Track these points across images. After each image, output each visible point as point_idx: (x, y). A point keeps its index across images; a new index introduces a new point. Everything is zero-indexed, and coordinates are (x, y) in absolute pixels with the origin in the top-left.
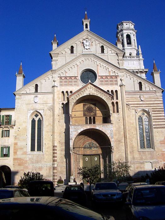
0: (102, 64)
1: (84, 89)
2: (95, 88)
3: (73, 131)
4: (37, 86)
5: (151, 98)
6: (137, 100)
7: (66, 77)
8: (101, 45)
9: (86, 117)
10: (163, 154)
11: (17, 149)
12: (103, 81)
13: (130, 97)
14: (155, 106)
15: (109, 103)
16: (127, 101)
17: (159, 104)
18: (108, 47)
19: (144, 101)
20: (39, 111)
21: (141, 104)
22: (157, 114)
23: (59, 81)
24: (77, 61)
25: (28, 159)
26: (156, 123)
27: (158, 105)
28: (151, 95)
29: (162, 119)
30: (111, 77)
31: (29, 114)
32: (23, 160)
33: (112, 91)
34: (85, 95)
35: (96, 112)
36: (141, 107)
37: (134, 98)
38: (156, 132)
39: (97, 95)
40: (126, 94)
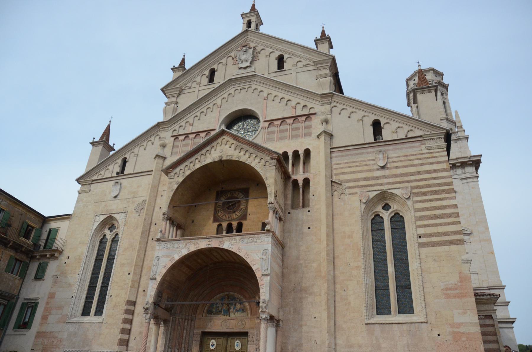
0: (274, 93)
1: (208, 148)
2: (234, 142)
3: (163, 256)
4: (125, 161)
5: (409, 158)
6: (366, 168)
7: (187, 135)
8: (277, 54)
9: (220, 226)
10: (458, 333)
11: (51, 310)
12: (273, 132)
13: (346, 161)
14: (422, 180)
15: (268, 175)
16: (337, 174)
17: (435, 171)
18: (295, 55)
19: (388, 168)
20: (114, 215)
21: (377, 178)
22: (431, 200)
23: (172, 145)
24: (219, 96)
25: (65, 336)
26: (429, 230)
27: (434, 175)
28: (410, 150)
29: (449, 215)
30: (295, 118)
31: (97, 224)
32: (55, 337)
33: (296, 154)
34: (208, 161)
35: (246, 209)
36: (378, 185)
37: (357, 164)
38: (426, 257)
39: (239, 157)
40: (334, 155)
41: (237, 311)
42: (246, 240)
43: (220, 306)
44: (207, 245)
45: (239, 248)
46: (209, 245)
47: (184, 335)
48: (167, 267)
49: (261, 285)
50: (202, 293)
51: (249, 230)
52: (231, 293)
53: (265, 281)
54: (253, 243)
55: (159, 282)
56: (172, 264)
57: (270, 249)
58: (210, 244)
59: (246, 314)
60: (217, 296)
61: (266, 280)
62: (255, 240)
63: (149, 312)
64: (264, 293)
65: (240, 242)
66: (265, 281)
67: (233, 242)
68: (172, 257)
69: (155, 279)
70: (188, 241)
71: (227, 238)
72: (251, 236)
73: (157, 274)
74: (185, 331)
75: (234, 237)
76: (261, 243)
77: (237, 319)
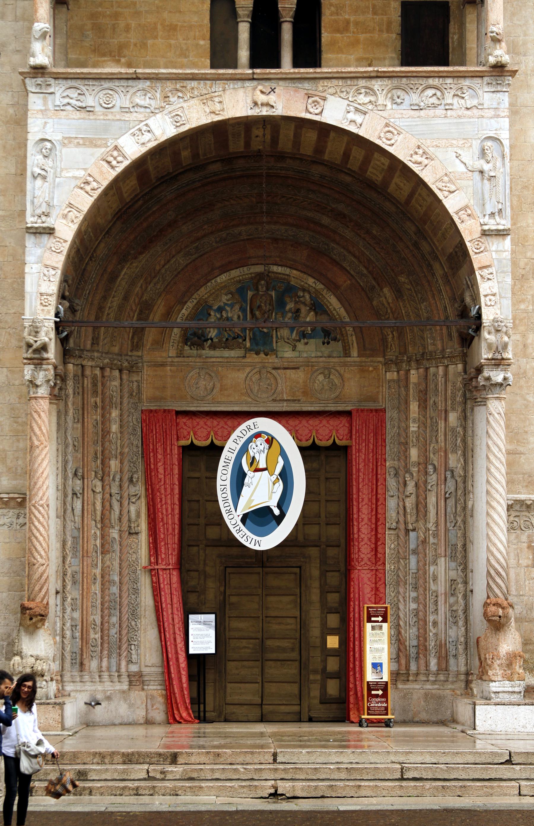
3: (67, 141)
41: (304, 335)
42: (414, 98)
44: (256, 104)
45: (387, 125)
46: (262, 105)
47: (114, 428)
48: (94, 185)
49: (480, 268)
50: (163, 266)
51: (352, 27)
52: (275, 268)
53: (494, 253)
54: (440, 111)
55: (67, 246)
56: (114, 174)
57: (505, 136)
58: (267, 105)
59: (341, 349)
61: (496, 251)
62: (449, 99)
63: (48, 359)
64: (494, 295)
65: (389, 106)
66: (494, 253)
67: (363, 99)
68: (111, 144)
69: (50, 231)
70: (170, 85)
71: (335, 82)
72: (431, 81)
73: (54, 213)
74: (115, 413)
75: (362, 83)
76: (468, 113)
77: (308, 364)
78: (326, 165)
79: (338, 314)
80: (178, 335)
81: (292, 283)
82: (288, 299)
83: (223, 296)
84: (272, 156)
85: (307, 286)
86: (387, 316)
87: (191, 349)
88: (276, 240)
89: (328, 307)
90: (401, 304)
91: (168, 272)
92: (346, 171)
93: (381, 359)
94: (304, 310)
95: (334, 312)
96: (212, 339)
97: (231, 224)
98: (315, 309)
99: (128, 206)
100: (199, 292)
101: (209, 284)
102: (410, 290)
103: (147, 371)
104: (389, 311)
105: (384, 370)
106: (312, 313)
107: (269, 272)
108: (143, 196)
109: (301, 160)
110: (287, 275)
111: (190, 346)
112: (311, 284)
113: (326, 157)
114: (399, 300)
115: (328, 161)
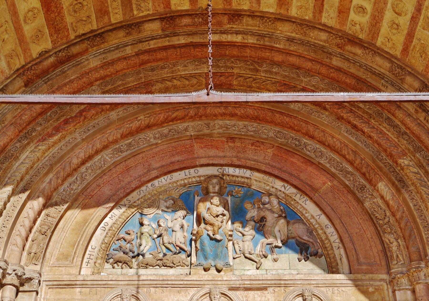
43: (177, 228)
50: (83, 163)
52: (231, 171)
60: (156, 182)
78: (294, 22)
79: (318, 223)
80: (96, 250)
81: (253, 187)
82: (248, 206)
83: (162, 202)
84: (225, 14)
85: (274, 190)
86: (387, 220)
87: (113, 268)
88: (232, 139)
89: (303, 215)
90: (407, 196)
91: (90, 171)
92: (321, 27)
93: (385, 276)
94: (270, 218)
95: (312, 221)
96: (143, 255)
97: (174, 115)
98: (285, 217)
99: (34, 63)
100: (129, 197)
101: (144, 188)
102: (418, 173)
103: (46, 293)
104: (388, 214)
105: (390, 290)
106: (282, 221)
107: (223, 175)
108: (55, 53)
109: (262, 17)
110: (247, 178)
111: (112, 264)
112: (279, 188)
113: (294, 12)
114: (403, 191)
115: (296, 18)
